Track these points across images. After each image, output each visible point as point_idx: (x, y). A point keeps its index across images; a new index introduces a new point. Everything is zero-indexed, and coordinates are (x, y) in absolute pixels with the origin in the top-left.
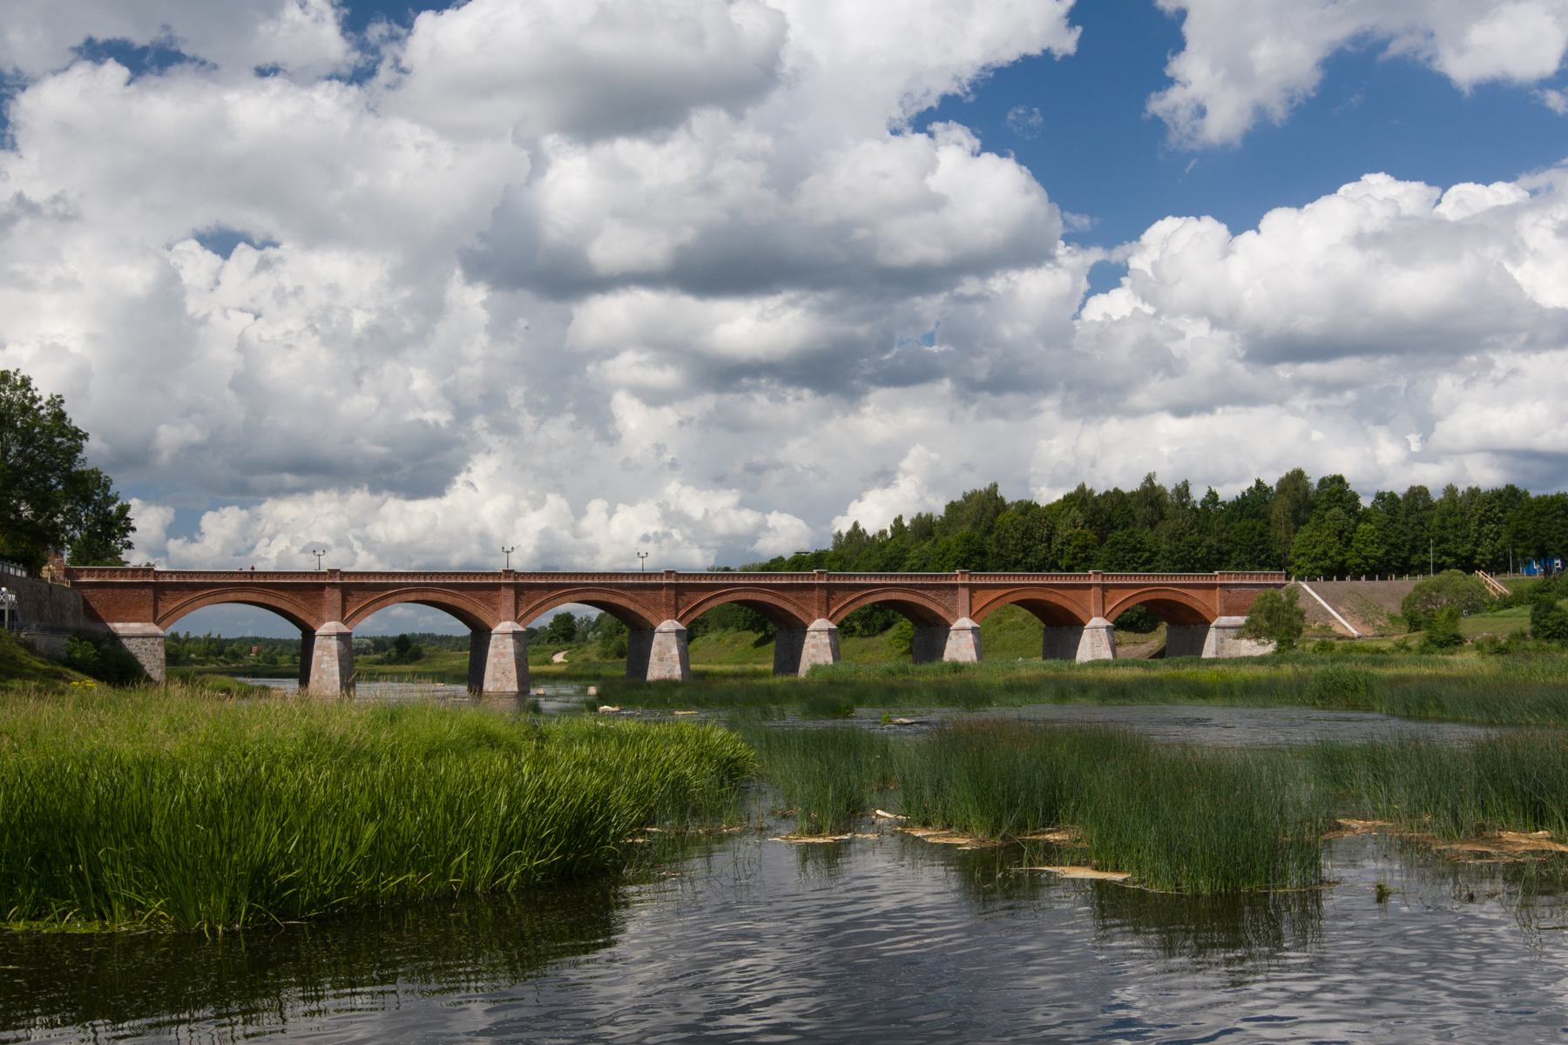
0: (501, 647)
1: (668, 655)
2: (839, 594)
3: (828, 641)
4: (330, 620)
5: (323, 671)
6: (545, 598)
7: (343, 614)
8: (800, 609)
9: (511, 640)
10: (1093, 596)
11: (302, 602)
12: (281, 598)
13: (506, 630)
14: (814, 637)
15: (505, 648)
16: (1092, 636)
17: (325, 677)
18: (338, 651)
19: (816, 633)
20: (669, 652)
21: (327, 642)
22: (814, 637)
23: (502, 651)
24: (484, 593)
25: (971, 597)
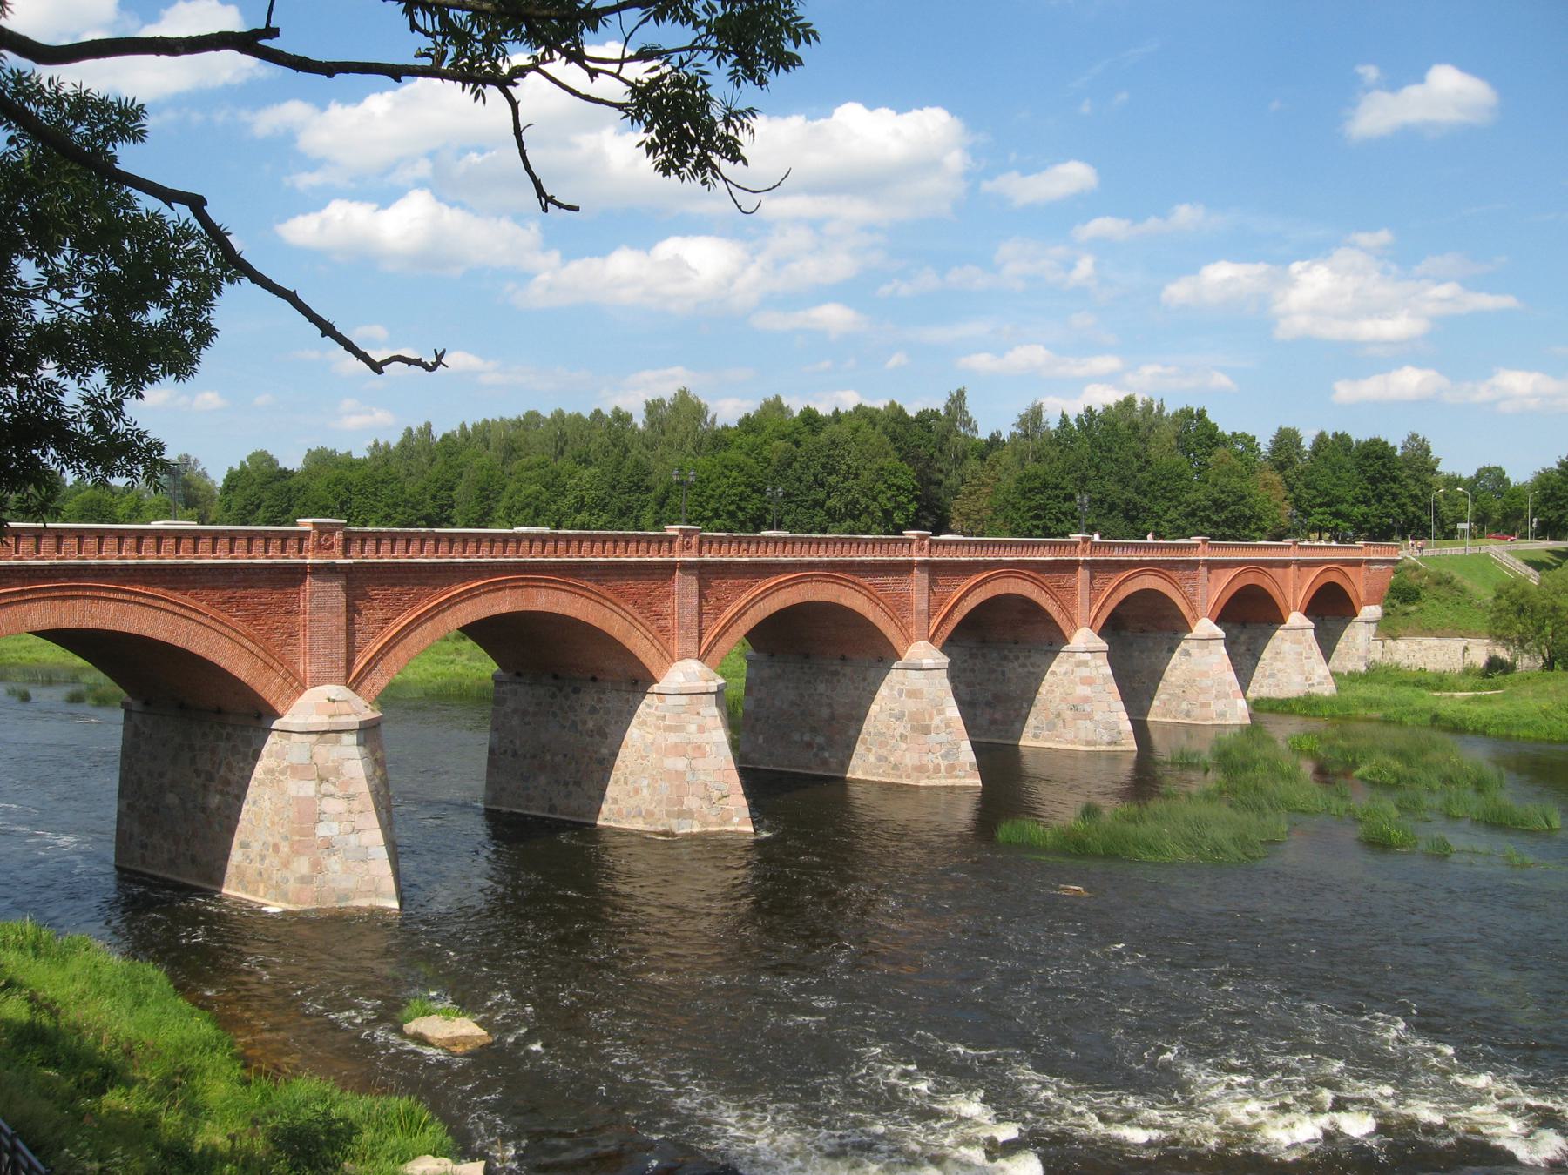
0: (693, 728)
1: (937, 721)
2: (722, 585)
3: (1109, 671)
4: (319, 680)
5: (329, 846)
6: (745, 598)
7: (350, 662)
8: (1063, 608)
9: (715, 711)
10: (917, 587)
11: (243, 627)
12: (184, 613)
13: (700, 686)
14: (1085, 664)
15: (701, 729)
16: (1294, 642)
17: (334, 864)
18: (369, 780)
19: (1087, 656)
20: (941, 712)
21: (328, 753)
22: (1085, 664)
23: (697, 738)
24: (637, 587)
25: (352, 610)
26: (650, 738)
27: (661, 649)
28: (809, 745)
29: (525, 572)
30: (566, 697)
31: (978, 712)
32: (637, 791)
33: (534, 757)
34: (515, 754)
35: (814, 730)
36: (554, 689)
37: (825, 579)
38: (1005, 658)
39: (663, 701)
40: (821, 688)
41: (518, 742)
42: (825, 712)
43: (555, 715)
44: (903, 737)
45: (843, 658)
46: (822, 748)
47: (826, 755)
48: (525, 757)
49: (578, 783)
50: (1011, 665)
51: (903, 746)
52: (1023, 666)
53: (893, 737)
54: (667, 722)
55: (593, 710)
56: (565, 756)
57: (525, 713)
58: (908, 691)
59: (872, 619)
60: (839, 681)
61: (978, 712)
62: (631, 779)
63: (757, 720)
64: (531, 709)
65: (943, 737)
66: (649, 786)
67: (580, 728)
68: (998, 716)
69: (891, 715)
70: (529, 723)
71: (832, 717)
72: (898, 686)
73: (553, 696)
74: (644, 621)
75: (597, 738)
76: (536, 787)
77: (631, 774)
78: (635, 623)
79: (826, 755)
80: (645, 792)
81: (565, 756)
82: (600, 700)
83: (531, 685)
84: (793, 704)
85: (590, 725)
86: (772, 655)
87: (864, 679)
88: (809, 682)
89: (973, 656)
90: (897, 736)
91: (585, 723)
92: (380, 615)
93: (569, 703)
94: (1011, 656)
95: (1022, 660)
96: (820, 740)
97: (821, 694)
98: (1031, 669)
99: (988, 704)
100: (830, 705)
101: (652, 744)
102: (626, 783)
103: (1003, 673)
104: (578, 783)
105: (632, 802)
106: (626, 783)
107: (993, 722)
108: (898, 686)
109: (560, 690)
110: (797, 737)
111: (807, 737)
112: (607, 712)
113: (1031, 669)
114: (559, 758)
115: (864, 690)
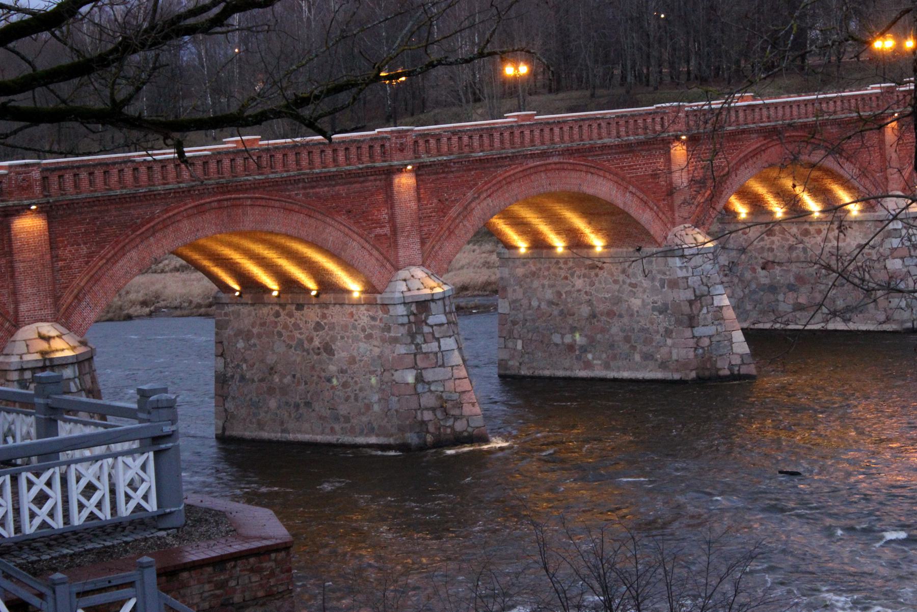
26: (377, 351)
27: (381, 258)
29: (229, 192)
30: (290, 315)
31: (781, 297)
32: (368, 407)
33: (262, 380)
34: (243, 378)
36: (277, 308)
37: (560, 168)
39: (387, 312)
40: (579, 283)
42: (585, 310)
44: (668, 333)
46: (584, 349)
47: (590, 356)
48: (253, 381)
49: (308, 404)
50: (813, 241)
51: (669, 342)
53: (658, 332)
54: (392, 334)
56: (294, 376)
58: (670, 281)
59: (621, 206)
60: (597, 275)
61: (781, 297)
62: (361, 395)
63: (514, 323)
64: (255, 331)
65: (711, 330)
66: (380, 400)
67: (306, 345)
68: (802, 300)
69: (654, 309)
71: (593, 316)
72: (659, 276)
73: (277, 315)
74: (360, 231)
75: (325, 356)
76: (266, 412)
77: (361, 390)
78: (350, 233)
79: (590, 356)
80: (376, 408)
81: (294, 376)
82: (324, 316)
83: (253, 305)
84: (551, 303)
85: (317, 342)
88: (566, 278)
90: (662, 330)
91: (311, 340)
92: (84, 250)
93: (293, 320)
97: (579, 291)
99: (791, 288)
100: (589, 302)
101: (379, 357)
102: (356, 399)
105: (364, 419)
106: (356, 399)
108: (659, 276)
110: (556, 339)
111: (568, 339)
112: (332, 327)
114: (287, 380)
115: (624, 282)
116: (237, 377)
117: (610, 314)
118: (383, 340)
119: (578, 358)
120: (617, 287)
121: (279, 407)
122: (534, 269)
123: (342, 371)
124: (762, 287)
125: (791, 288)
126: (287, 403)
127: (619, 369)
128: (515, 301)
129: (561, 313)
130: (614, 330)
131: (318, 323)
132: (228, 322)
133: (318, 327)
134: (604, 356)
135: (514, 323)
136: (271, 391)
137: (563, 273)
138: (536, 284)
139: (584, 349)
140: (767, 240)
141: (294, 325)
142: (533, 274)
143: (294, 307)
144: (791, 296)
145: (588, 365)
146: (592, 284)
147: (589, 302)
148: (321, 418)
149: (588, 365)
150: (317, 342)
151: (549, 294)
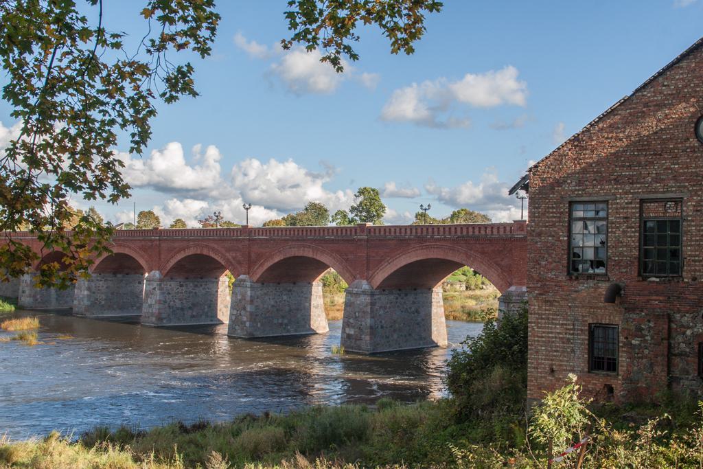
28: (281, 324)
30: (402, 298)
31: (186, 312)
33: (391, 327)
34: (382, 327)
35: (283, 317)
36: (397, 296)
38: (196, 286)
40: (285, 297)
41: (383, 322)
42: (287, 308)
43: (398, 306)
45: (294, 283)
46: (286, 325)
49: (410, 335)
51: (319, 319)
52: (204, 289)
55: (414, 303)
57: (385, 308)
63: (257, 315)
68: (194, 313)
70: (387, 312)
71: (290, 310)
73: (397, 299)
75: (416, 314)
79: (289, 327)
82: (416, 298)
84: (273, 306)
85: (413, 309)
86: (263, 284)
87: (302, 292)
89: (181, 286)
90: (317, 315)
91: (410, 308)
93: (404, 301)
94: (199, 285)
95: (203, 287)
96: (286, 321)
98: (207, 290)
100: (289, 306)
103: (196, 293)
104: (410, 335)
107: (193, 316)
109: (400, 296)
110: (275, 321)
111: (280, 321)
113: (207, 290)
116: (380, 327)
117: (298, 309)
118: (437, 306)
119: (284, 328)
120: (299, 299)
121: (398, 337)
122: (265, 291)
123: (423, 320)
124: (178, 309)
125: (190, 308)
126: (401, 335)
127: (300, 332)
128: (257, 306)
129: (277, 310)
130: (299, 316)
131: (413, 301)
132: (376, 303)
133: (414, 303)
134: (295, 327)
135: (257, 315)
136: (395, 331)
137: (278, 294)
138: (267, 298)
139: (286, 325)
140: (180, 290)
141: (405, 302)
142: (265, 294)
143: (403, 295)
144: (190, 311)
145: (288, 331)
146: (290, 298)
147: (289, 306)
148: (416, 340)
149: (288, 331)
150: (413, 309)
151: (272, 303)
